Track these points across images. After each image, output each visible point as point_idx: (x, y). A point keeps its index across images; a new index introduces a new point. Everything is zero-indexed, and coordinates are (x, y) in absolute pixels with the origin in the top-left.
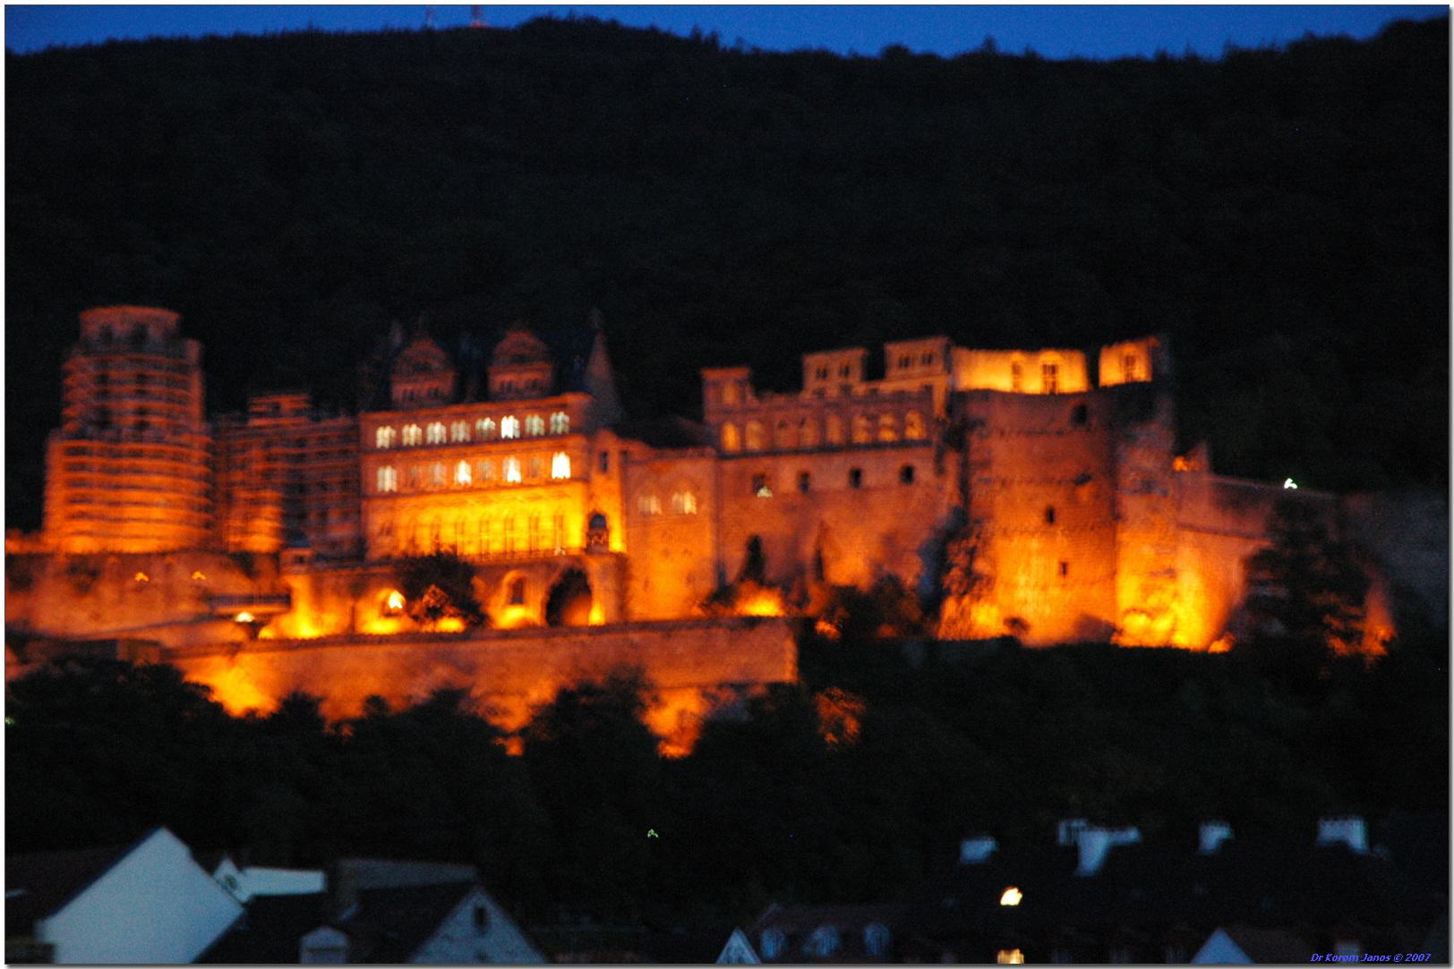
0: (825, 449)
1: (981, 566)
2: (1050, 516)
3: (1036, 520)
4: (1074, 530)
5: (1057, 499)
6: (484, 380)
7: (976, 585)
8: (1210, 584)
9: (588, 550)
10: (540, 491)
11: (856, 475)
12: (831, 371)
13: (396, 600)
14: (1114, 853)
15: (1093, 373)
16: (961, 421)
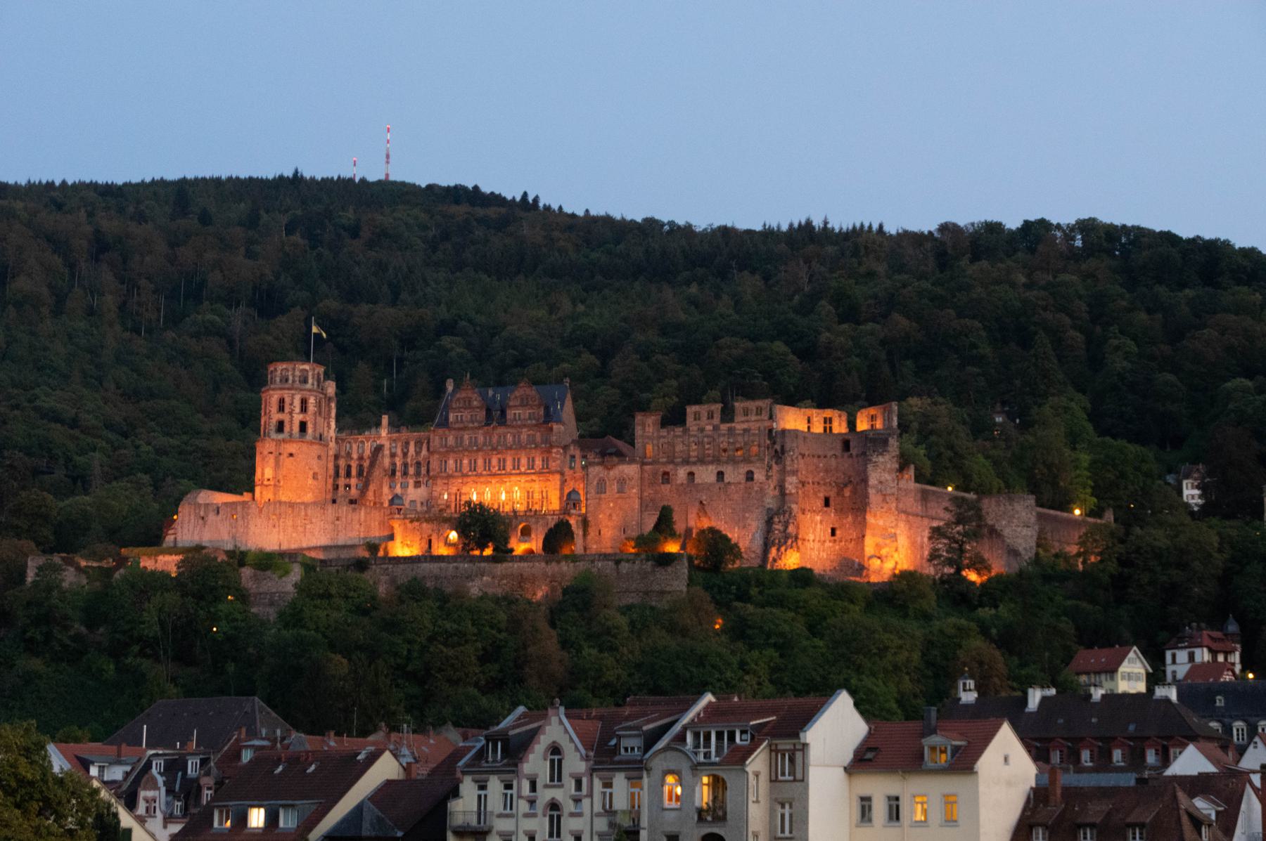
0: (702, 461)
1: (791, 529)
2: (827, 503)
3: (819, 503)
4: (841, 511)
5: (832, 494)
6: (503, 413)
7: (790, 539)
8: (913, 543)
9: (565, 511)
10: (534, 477)
11: (720, 475)
12: (701, 417)
13: (453, 535)
14: (1044, 699)
15: (852, 424)
16: (778, 446)
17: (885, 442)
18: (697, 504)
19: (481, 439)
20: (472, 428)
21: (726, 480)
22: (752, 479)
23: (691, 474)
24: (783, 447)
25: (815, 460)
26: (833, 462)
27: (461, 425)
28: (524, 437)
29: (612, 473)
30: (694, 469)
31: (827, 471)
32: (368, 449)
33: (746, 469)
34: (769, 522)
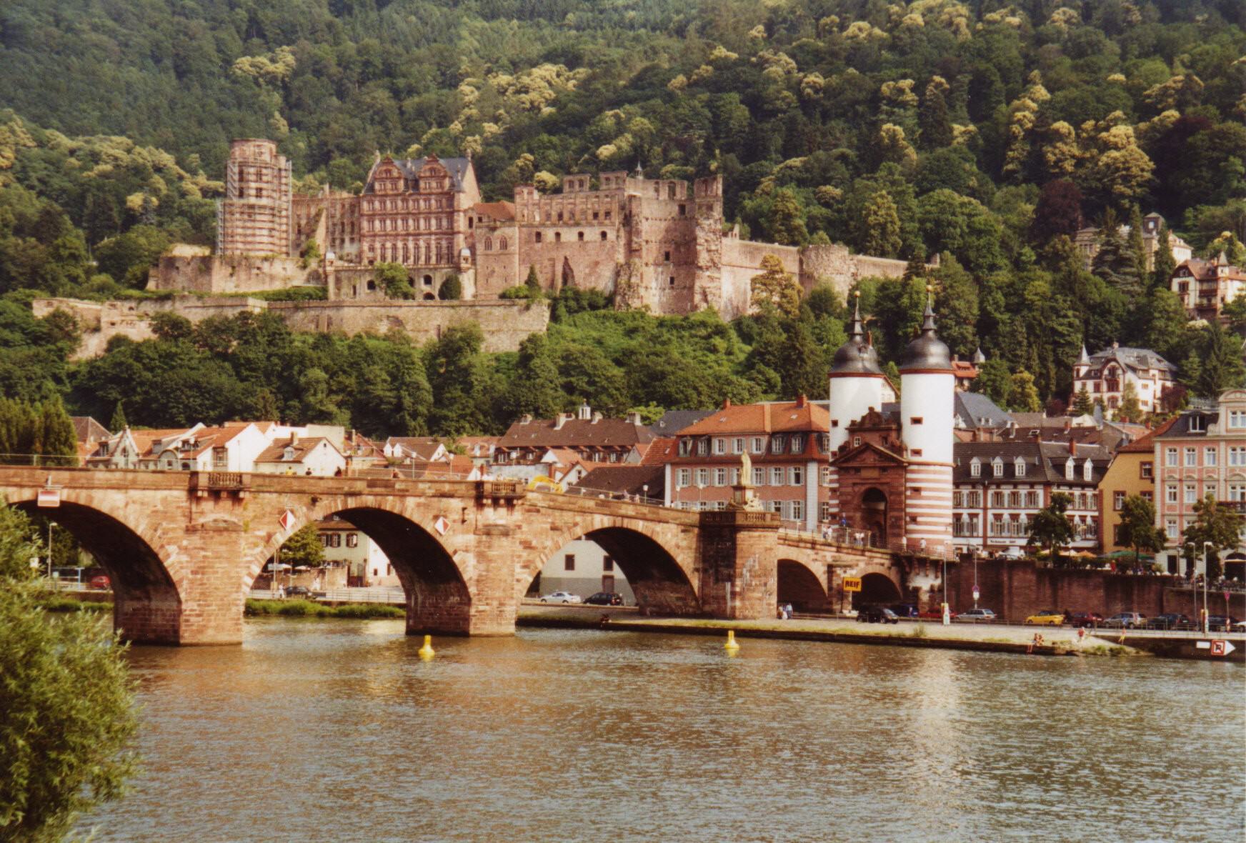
1: (633, 280)
2: (667, 256)
3: (661, 258)
4: (678, 265)
5: (671, 250)
11: (581, 235)
17: (710, 208)
23: (558, 235)
25: (658, 222)
28: (433, 202)
30: (559, 230)
32: (313, 211)
34: (618, 274)
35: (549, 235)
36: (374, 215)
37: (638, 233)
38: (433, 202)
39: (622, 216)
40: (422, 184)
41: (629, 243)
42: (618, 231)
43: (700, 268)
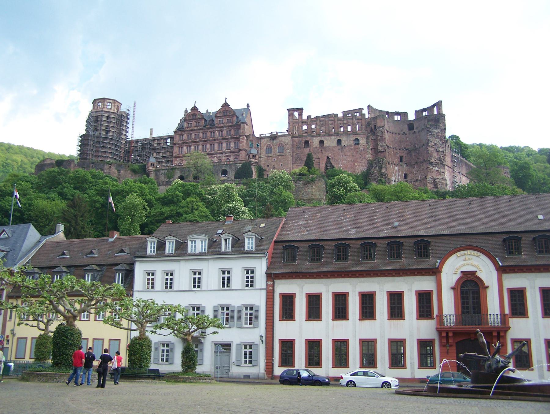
0: (329, 135)
1: (383, 170)
3: (397, 160)
5: (404, 154)
10: (230, 154)
11: (339, 142)
18: (326, 158)
19: (201, 135)
20: (196, 130)
21: (343, 145)
22: (358, 144)
23: (322, 142)
24: (375, 126)
25: (394, 135)
26: (404, 137)
27: (191, 129)
28: (225, 132)
29: (275, 142)
31: (400, 142)
33: (354, 138)
35: (315, 142)
36: (183, 143)
37: (383, 140)
38: (225, 132)
39: (369, 129)
40: (216, 121)
41: (375, 150)
42: (367, 139)
43: (432, 163)
